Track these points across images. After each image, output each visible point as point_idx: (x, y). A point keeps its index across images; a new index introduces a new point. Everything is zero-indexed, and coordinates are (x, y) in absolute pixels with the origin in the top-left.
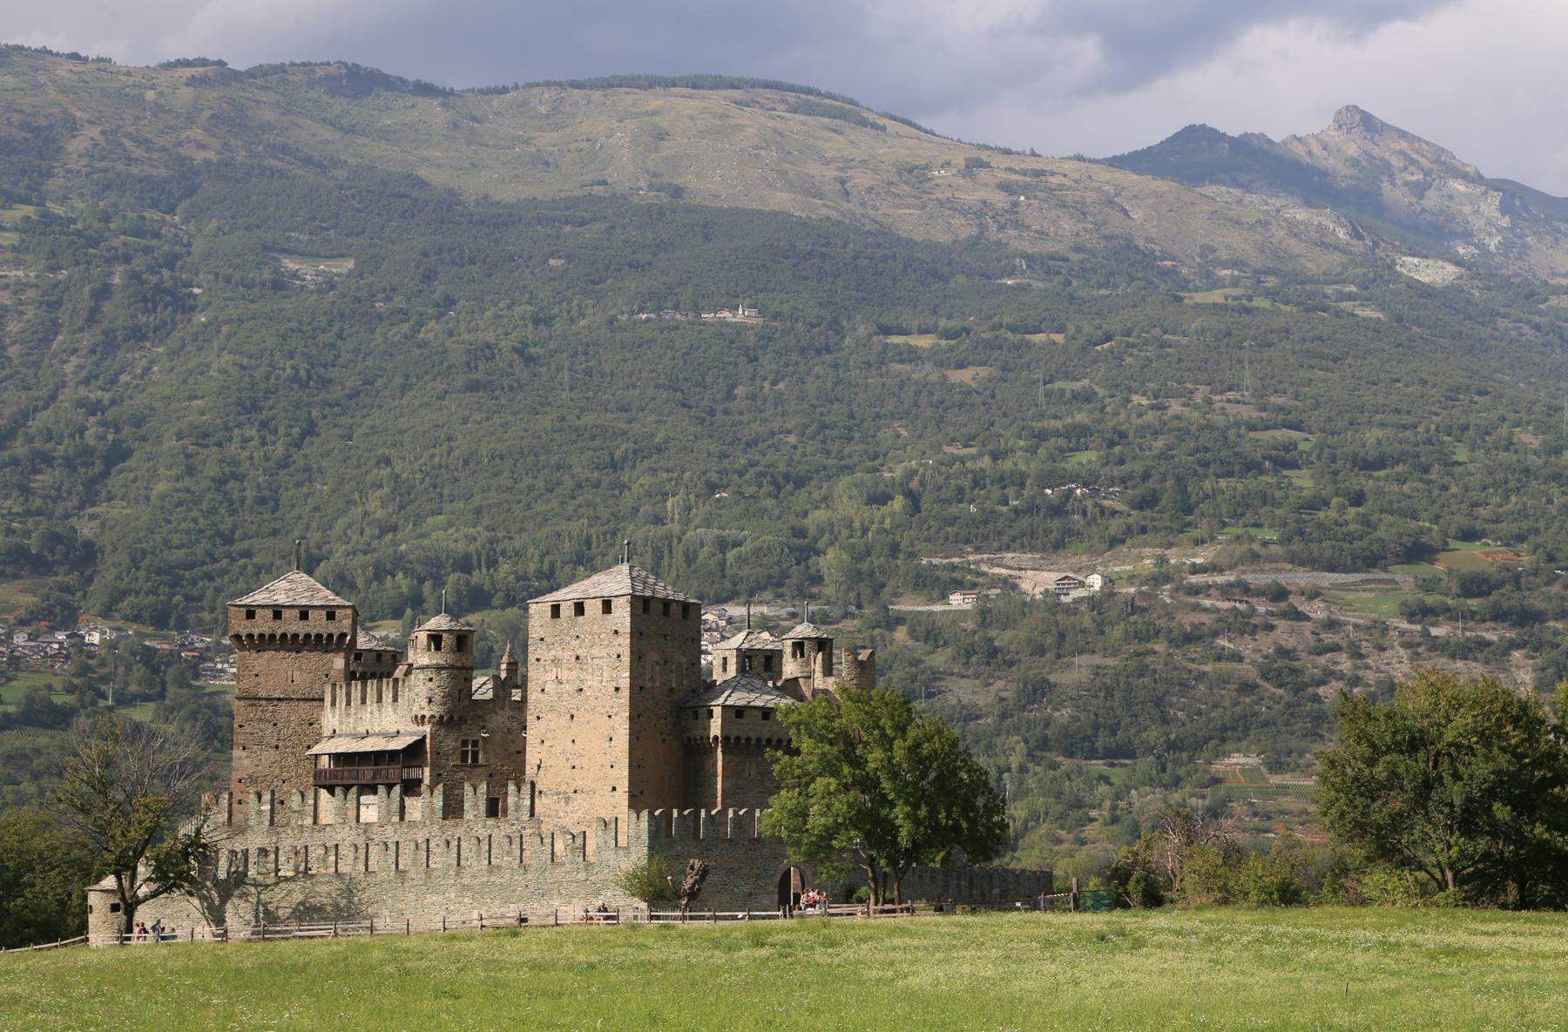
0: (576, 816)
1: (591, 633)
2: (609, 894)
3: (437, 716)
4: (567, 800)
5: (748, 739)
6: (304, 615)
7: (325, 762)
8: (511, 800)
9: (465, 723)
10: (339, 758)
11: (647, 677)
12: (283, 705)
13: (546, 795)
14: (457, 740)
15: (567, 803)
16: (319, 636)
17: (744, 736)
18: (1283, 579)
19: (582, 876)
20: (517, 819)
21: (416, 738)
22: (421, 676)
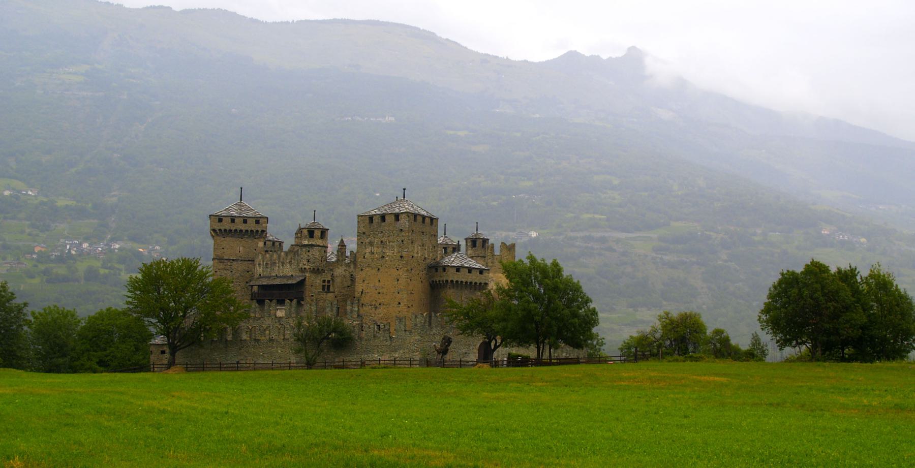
0: (380, 316)
1: (388, 231)
2: (401, 352)
3: (312, 268)
4: (376, 308)
5: (462, 282)
6: (245, 222)
7: (255, 289)
8: (349, 308)
9: (324, 272)
10: (261, 287)
11: (415, 251)
12: (235, 263)
13: (365, 306)
14: (320, 280)
15: (375, 310)
16: (252, 231)
17: (460, 280)
18: (606, 235)
19: (388, 343)
20: (352, 317)
21: (301, 278)
22: (304, 250)
